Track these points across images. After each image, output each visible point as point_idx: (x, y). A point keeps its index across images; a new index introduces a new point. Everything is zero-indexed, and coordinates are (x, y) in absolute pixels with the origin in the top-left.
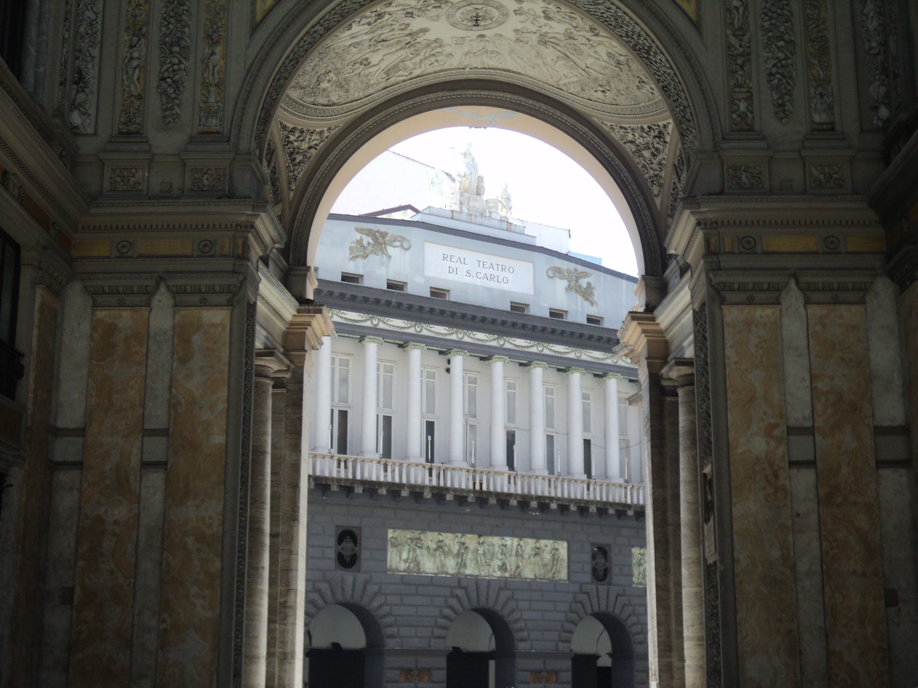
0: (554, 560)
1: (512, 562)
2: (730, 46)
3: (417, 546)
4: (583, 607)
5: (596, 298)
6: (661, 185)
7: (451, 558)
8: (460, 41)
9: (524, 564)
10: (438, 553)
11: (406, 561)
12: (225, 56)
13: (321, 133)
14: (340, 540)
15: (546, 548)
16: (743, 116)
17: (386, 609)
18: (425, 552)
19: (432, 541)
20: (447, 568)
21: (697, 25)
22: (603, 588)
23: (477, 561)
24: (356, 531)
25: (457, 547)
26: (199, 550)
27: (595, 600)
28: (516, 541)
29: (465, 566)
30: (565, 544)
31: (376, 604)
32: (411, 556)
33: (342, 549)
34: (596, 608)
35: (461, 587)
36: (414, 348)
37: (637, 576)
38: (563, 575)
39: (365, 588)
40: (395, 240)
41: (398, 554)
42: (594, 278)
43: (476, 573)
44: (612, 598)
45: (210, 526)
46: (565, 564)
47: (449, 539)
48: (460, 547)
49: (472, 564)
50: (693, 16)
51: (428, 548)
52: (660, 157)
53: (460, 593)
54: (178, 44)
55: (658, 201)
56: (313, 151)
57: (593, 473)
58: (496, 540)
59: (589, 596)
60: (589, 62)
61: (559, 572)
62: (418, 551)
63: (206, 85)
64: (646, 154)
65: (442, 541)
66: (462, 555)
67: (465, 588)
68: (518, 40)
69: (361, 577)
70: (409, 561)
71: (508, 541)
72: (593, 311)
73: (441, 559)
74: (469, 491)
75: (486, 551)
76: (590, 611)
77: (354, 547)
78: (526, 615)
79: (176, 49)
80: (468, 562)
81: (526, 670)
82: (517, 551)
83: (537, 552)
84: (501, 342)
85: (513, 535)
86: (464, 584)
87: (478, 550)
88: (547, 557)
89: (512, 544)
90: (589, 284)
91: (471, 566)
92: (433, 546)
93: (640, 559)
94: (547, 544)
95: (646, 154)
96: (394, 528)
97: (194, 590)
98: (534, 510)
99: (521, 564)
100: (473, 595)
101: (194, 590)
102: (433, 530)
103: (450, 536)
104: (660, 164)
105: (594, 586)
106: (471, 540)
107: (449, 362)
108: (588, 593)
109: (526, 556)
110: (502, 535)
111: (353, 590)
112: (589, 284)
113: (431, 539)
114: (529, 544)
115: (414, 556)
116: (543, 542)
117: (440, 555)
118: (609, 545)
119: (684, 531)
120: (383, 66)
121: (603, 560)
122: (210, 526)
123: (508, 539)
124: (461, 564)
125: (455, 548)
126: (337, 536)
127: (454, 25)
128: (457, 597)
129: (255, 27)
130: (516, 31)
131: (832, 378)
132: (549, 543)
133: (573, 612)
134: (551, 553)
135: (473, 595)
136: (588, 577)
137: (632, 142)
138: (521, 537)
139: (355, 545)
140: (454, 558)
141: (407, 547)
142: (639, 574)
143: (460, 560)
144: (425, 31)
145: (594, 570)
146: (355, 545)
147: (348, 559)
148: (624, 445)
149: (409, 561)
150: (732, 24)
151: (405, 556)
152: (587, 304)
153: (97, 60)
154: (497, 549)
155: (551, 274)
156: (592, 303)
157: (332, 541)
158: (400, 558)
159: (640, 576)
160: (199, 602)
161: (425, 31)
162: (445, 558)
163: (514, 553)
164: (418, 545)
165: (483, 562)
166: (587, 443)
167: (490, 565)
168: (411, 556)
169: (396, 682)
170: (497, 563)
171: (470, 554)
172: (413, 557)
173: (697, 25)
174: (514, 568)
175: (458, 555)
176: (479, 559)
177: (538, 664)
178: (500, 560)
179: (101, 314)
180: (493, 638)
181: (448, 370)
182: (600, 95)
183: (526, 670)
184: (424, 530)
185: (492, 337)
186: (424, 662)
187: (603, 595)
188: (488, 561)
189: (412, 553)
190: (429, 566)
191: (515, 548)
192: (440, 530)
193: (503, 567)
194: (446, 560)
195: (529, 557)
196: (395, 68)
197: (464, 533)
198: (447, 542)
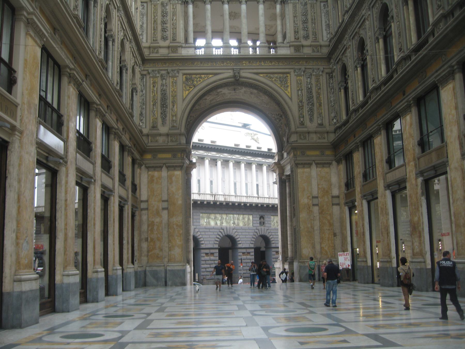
1: (236, 221)
2: (299, 104)
5: (259, 142)
6: (281, 128)
8: (230, 93)
11: (206, 222)
12: (177, 108)
13: (193, 117)
16: (302, 122)
17: (201, 236)
18: (211, 219)
21: (291, 99)
22: (263, 228)
26: (177, 228)
27: (260, 231)
28: (237, 216)
29: (223, 223)
30: (252, 216)
34: (261, 234)
35: (222, 229)
38: (251, 224)
42: (259, 135)
43: (226, 225)
44: (265, 231)
45: (179, 223)
47: (218, 216)
50: (290, 96)
51: (212, 219)
52: (281, 121)
53: (222, 231)
54: (165, 104)
55: (281, 132)
56: (191, 121)
57: (259, 194)
58: (232, 216)
60: (263, 98)
61: (250, 224)
63: (173, 116)
64: (278, 120)
67: (223, 229)
68: (245, 93)
71: (235, 216)
72: (259, 146)
74: (224, 201)
76: (259, 235)
78: (241, 236)
79: (165, 106)
80: (224, 222)
81: (241, 252)
83: (243, 218)
85: (236, 214)
86: (222, 228)
88: (246, 219)
90: (257, 138)
92: (213, 218)
94: (246, 216)
95: (278, 120)
96: (202, 213)
97: (176, 238)
98: (242, 206)
100: (226, 231)
101: (176, 238)
102: (213, 213)
104: (281, 123)
106: (224, 216)
107: (216, 162)
110: (233, 214)
112: (257, 138)
113: (212, 216)
116: (245, 216)
118: (264, 215)
119: (288, 218)
120: (210, 100)
121: (262, 220)
122: (179, 223)
125: (220, 218)
127: (229, 90)
128: (221, 232)
129: (184, 100)
130: (244, 91)
131: (322, 185)
132: (247, 216)
135: (226, 231)
136: (258, 225)
137: (274, 117)
138: (238, 214)
141: (206, 218)
144: (221, 92)
145: (260, 223)
148: (268, 185)
150: (299, 99)
151: (205, 221)
152: (257, 143)
153: (145, 109)
155: (246, 135)
156: (258, 143)
160: (178, 240)
161: (221, 92)
166: (257, 185)
169: (204, 257)
170: (232, 222)
173: (291, 99)
175: (220, 220)
177: (244, 251)
179: (150, 173)
180: (231, 243)
181: (216, 165)
182: (265, 106)
183: (241, 252)
184: (211, 213)
185: (229, 155)
186: (212, 251)
187: (263, 230)
190: (212, 223)
192: (215, 213)
193: (234, 223)
196: (213, 100)
197: (222, 214)
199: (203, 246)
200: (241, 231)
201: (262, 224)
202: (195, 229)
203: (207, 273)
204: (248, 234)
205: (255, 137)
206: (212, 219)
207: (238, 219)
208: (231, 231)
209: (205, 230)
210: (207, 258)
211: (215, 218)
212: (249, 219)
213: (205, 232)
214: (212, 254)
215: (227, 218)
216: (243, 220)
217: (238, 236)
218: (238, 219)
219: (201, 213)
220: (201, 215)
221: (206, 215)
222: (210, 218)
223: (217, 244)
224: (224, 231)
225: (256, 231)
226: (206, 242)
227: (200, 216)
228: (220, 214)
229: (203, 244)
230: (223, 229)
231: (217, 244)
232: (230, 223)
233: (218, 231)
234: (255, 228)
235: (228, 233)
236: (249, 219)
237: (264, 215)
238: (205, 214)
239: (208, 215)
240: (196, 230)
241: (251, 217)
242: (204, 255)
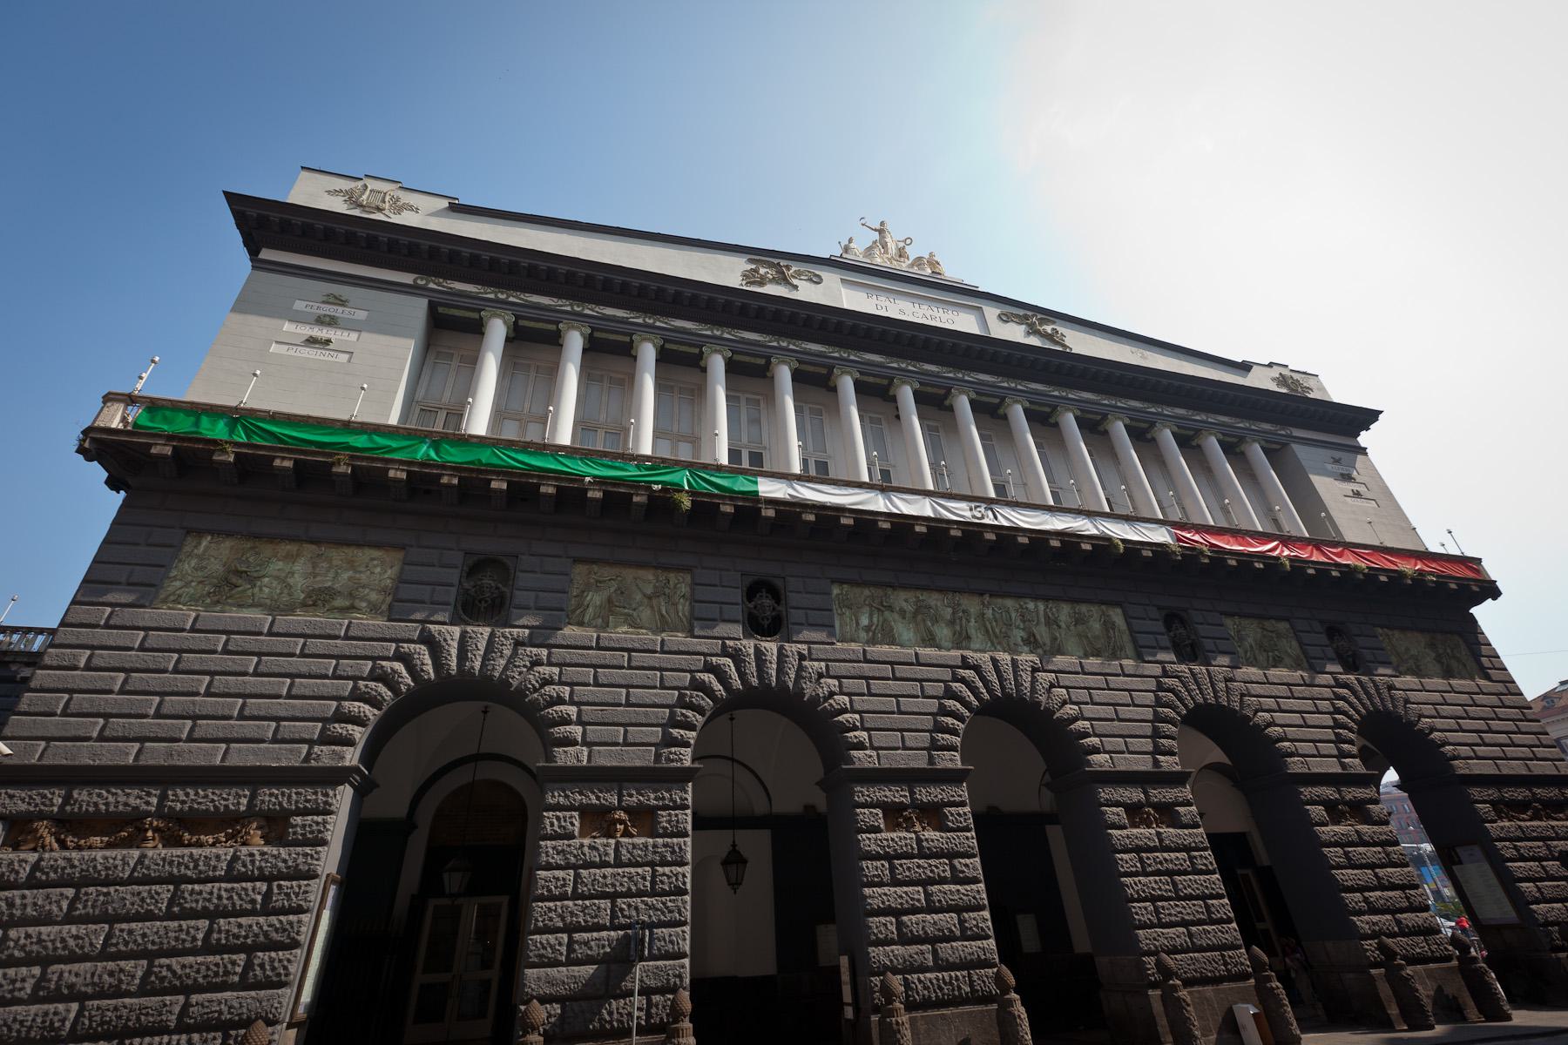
0: (1107, 631)
3: (883, 606)
4: (1181, 700)
7: (944, 625)
9: (1063, 636)
10: (920, 617)
14: (752, 592)
15: (1091, 613)
18: (896, 616)
19: (906, 601)
20: (941, 640)
23: (987, 631)
24: (779, 583)
25: (950, 610)
28: (1041, 606)
32: (875, 620)
33: (755, 607)
36: (842, 373)
37: (1243, 655)
39: (801, 668)
40: (799, 275)
41: (853, 618)
46: (1126, 637)
48: (953, 608)
49: (979, 634)
62: (887, 614)
65: (923, 601)
66: (961, 619)
69: (792, 648)
70: (874, 627)
71: (1031, 605)
73: (925, 625)
75: (997, 616)
77: (776, 605)
78: (1089, 710)
80: (972, 632)
82: (1046, 613)
83: (1079, 620)
84: (960, 375)
85: (1036, 598)
87: (984, 614)
88: (1096, 626)
89: (1036, 607)
91: (977, 637)
92: (909, 608)
93: (1238, 631)
94: (1092, 612)
96: (841, 582)
99: (1058, 635)
102: (905, 587)
103: (936, 595)
106: (972, 605)
109: (1063, 625)
110: (1018, 596)
113: (903, 600)
114: (1064, 612)
115: (881, 619)
116: (1084, 608)
117: (924, 620)
123: (1027, 600)
124: (960, 634)
126: (745, 589)
128: (963, 680)
132: (1095, 610)
134: (1100, 620)
138: (1046, 599)
139: (778, 602)
140: (947, 625)
142: (1246, 652)
143: (958, 628)
146: (778, 602)
147: (766, 623)
149: (874, 627)
151: (865, 621)
154: (1013, 615)
157: (737, 595)
158: (857, 624)
159: (1249, 654)
162: (933, 625)
163: (1043, 620)
164: (885, 604)
165: (997, 631)
167: (1009, 637)
168: (875, 620)
171: (973, 620)
172: (878, 621)
174: (1048, 642)
176: (989, 627)
178: (1023, 629)
181: (898, 417)
188: (1003, 630)
189: (876, 616)
191: (1042, 613)
194: (935, 627)
195: (1068, 627)
198: (933, 603)
199: (863, 759)
203: (913, 949)
204: (1124, 697)
205: (1048, 329)
206: (902, 613)
207: (1051, 622)
208: (1026, 678)
209: (866, 668)
210: (900, 838)
211: (920, 610)
212: (1108, 625)
213: (867, 678)
214: (933, 814)
215: (989, 613)
216: (1080, 628)
217: (1071, 710)
218: (1051, 622)
219: (833, 581)
220: (836, 591)
221: (867, 592)
222: (890, 608)
226: (880, 738)
227: (829, 594)
228: (940, 590)
229: (860, 746)
232: (1007, 636)
233: (946, 674)
236: (1108, 625)
238: (857, 590)
239: (879, 592)
241: (1117, 616)
242: (876, 817)
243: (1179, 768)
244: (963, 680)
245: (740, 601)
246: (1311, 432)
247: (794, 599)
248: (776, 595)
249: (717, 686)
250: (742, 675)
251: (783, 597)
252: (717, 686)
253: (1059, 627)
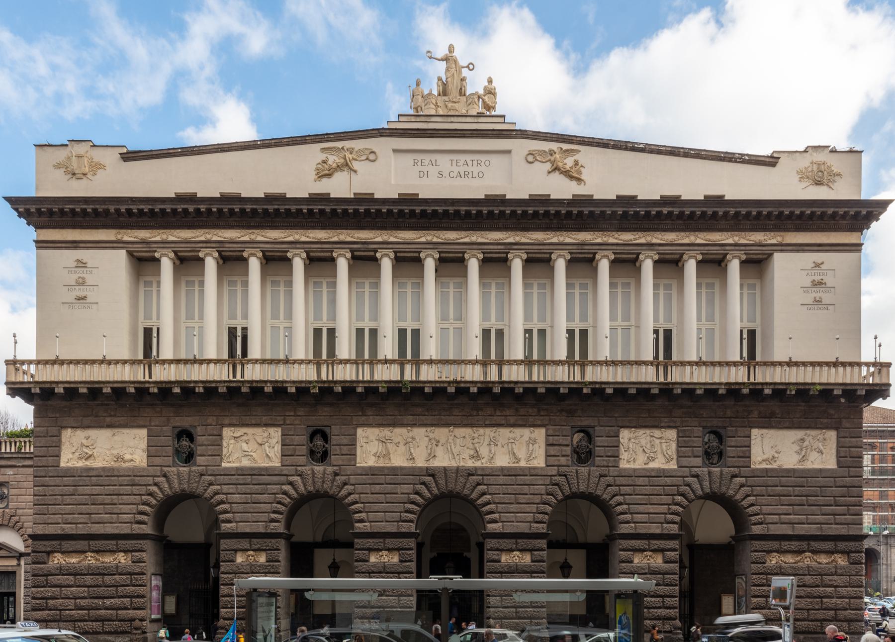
14: (312, 437)
31: (343, 492)
44: (594, 480)
59: (567, 479)
69: (330, 469)
100: (442, 482)
105: (573, 469)
108: (565, 476)
111: (323, 482)
118: (593, 427)
124: (430, 454)
126: (308, 435)
128: (423, 483)
133: (548, 494)
200: (502, 479)
201: (583, 456)
202: (336, 474)
223: (411, 521)
224: (436, 482)
225: (558, 478)
230: (433, 475)
231: (411, 521)
234: (554, 471)
235: (451, 486)
237: (593, 427)
240: (338, 478)
243: (545, 531)
244: (423, 483)
245: (305, 443)
246: (819, 234)
247: (334, 439)
248: (325, 437)
249: (292, 492)
250: (305, 485)
251: (329, 439)
252: (292, 492)
253: (497, 445)
